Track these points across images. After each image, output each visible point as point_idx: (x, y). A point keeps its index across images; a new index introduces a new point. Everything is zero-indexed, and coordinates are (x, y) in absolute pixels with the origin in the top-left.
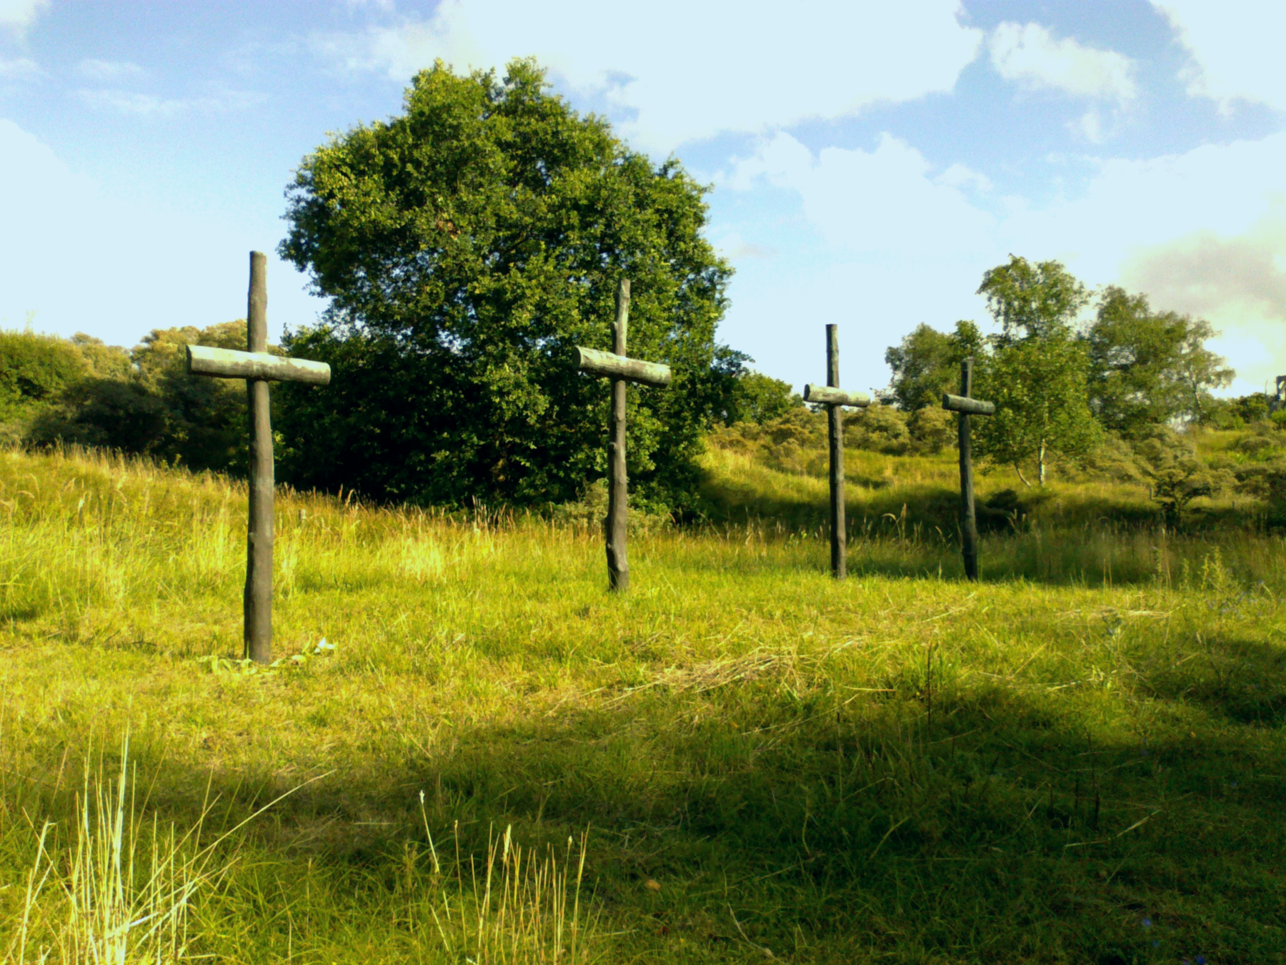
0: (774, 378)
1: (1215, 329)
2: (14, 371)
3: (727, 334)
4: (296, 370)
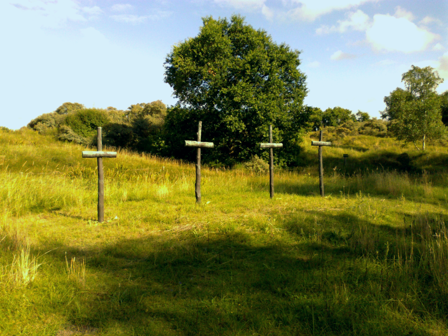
0: (345, 108)
2: (89, 121)
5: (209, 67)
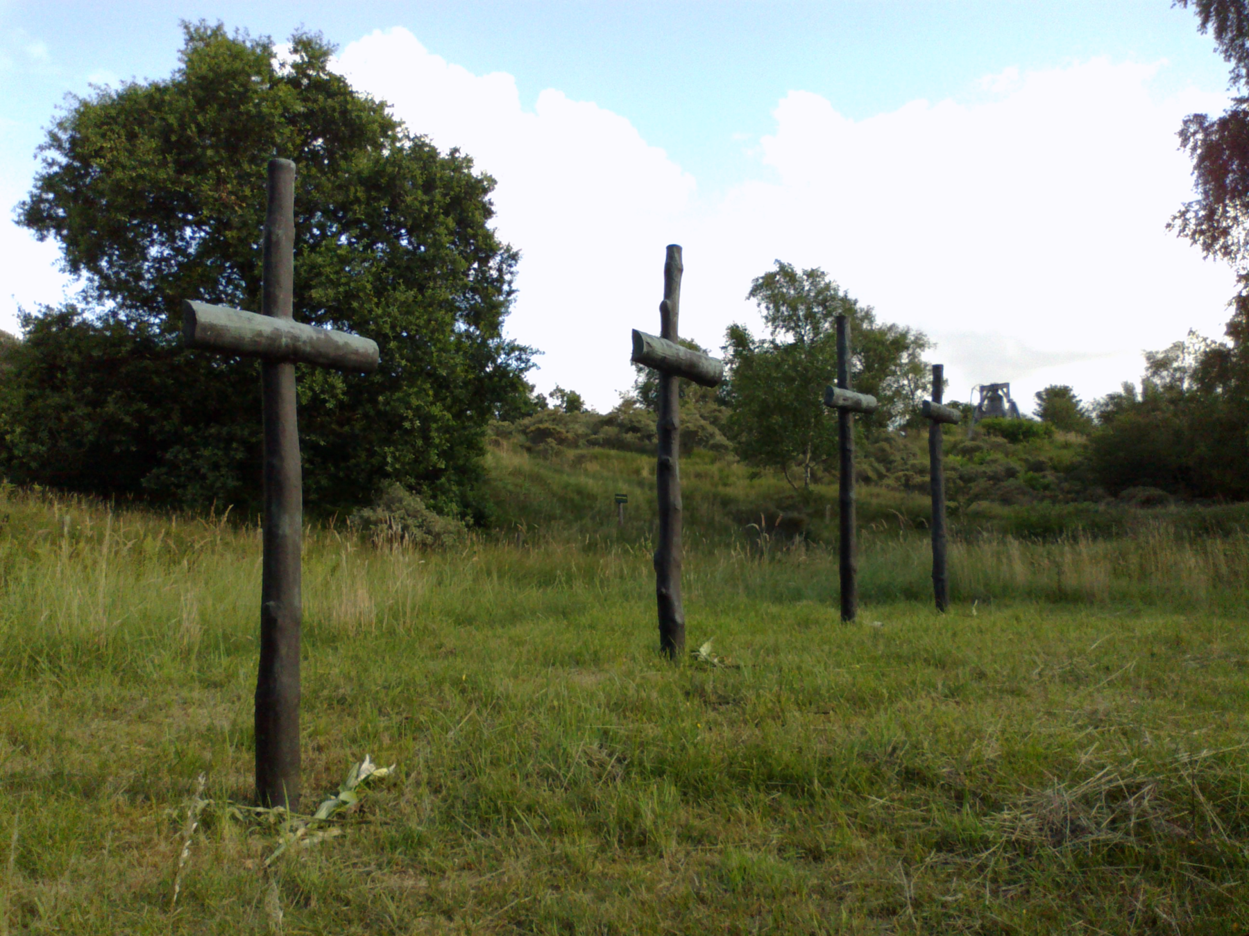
1: (932, 340)
3: (512, 328)
4: (337, 347)
5: (220, 181)
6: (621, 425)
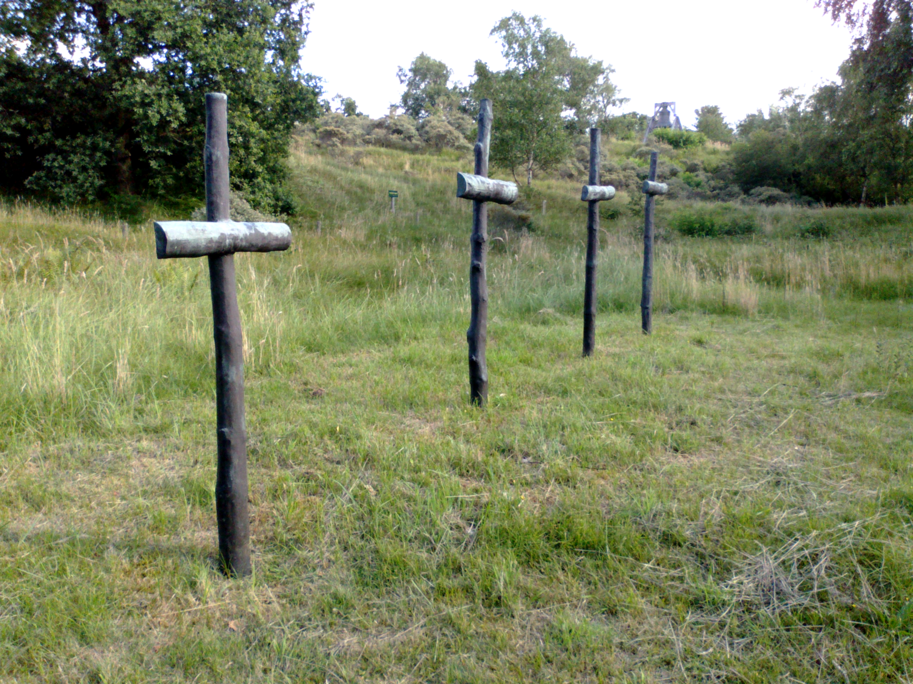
6: (388, 128)
